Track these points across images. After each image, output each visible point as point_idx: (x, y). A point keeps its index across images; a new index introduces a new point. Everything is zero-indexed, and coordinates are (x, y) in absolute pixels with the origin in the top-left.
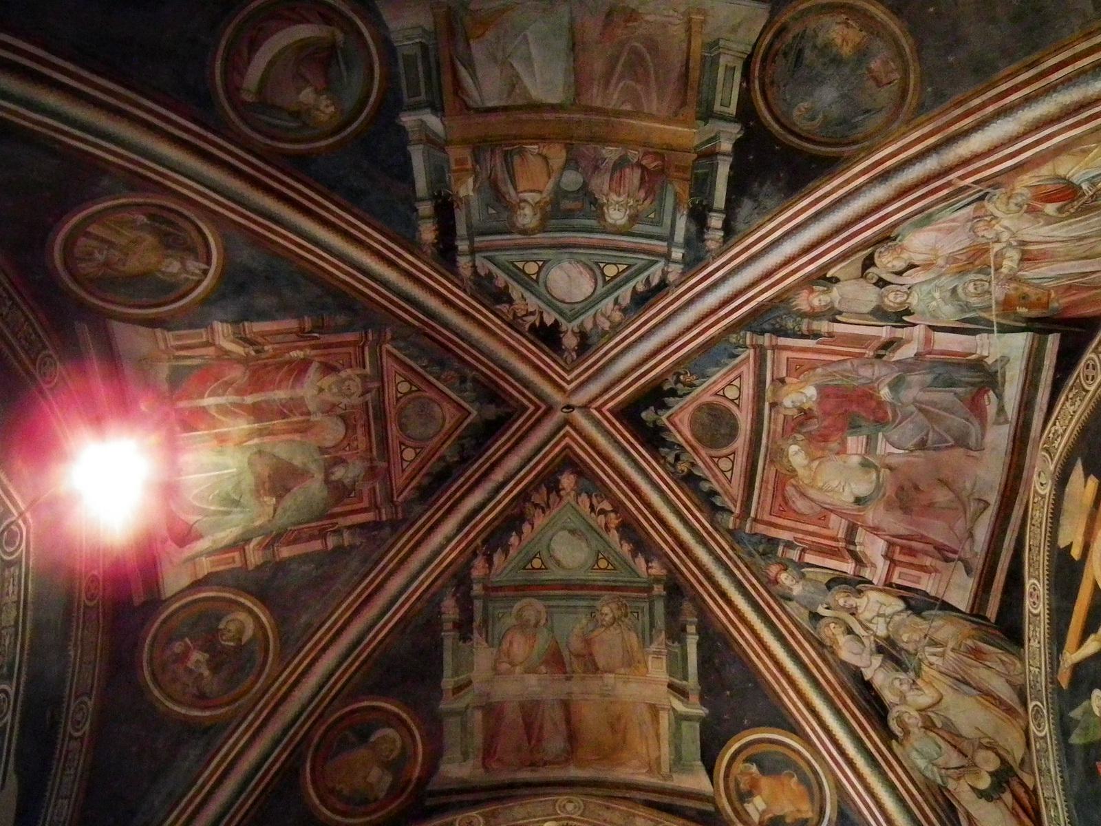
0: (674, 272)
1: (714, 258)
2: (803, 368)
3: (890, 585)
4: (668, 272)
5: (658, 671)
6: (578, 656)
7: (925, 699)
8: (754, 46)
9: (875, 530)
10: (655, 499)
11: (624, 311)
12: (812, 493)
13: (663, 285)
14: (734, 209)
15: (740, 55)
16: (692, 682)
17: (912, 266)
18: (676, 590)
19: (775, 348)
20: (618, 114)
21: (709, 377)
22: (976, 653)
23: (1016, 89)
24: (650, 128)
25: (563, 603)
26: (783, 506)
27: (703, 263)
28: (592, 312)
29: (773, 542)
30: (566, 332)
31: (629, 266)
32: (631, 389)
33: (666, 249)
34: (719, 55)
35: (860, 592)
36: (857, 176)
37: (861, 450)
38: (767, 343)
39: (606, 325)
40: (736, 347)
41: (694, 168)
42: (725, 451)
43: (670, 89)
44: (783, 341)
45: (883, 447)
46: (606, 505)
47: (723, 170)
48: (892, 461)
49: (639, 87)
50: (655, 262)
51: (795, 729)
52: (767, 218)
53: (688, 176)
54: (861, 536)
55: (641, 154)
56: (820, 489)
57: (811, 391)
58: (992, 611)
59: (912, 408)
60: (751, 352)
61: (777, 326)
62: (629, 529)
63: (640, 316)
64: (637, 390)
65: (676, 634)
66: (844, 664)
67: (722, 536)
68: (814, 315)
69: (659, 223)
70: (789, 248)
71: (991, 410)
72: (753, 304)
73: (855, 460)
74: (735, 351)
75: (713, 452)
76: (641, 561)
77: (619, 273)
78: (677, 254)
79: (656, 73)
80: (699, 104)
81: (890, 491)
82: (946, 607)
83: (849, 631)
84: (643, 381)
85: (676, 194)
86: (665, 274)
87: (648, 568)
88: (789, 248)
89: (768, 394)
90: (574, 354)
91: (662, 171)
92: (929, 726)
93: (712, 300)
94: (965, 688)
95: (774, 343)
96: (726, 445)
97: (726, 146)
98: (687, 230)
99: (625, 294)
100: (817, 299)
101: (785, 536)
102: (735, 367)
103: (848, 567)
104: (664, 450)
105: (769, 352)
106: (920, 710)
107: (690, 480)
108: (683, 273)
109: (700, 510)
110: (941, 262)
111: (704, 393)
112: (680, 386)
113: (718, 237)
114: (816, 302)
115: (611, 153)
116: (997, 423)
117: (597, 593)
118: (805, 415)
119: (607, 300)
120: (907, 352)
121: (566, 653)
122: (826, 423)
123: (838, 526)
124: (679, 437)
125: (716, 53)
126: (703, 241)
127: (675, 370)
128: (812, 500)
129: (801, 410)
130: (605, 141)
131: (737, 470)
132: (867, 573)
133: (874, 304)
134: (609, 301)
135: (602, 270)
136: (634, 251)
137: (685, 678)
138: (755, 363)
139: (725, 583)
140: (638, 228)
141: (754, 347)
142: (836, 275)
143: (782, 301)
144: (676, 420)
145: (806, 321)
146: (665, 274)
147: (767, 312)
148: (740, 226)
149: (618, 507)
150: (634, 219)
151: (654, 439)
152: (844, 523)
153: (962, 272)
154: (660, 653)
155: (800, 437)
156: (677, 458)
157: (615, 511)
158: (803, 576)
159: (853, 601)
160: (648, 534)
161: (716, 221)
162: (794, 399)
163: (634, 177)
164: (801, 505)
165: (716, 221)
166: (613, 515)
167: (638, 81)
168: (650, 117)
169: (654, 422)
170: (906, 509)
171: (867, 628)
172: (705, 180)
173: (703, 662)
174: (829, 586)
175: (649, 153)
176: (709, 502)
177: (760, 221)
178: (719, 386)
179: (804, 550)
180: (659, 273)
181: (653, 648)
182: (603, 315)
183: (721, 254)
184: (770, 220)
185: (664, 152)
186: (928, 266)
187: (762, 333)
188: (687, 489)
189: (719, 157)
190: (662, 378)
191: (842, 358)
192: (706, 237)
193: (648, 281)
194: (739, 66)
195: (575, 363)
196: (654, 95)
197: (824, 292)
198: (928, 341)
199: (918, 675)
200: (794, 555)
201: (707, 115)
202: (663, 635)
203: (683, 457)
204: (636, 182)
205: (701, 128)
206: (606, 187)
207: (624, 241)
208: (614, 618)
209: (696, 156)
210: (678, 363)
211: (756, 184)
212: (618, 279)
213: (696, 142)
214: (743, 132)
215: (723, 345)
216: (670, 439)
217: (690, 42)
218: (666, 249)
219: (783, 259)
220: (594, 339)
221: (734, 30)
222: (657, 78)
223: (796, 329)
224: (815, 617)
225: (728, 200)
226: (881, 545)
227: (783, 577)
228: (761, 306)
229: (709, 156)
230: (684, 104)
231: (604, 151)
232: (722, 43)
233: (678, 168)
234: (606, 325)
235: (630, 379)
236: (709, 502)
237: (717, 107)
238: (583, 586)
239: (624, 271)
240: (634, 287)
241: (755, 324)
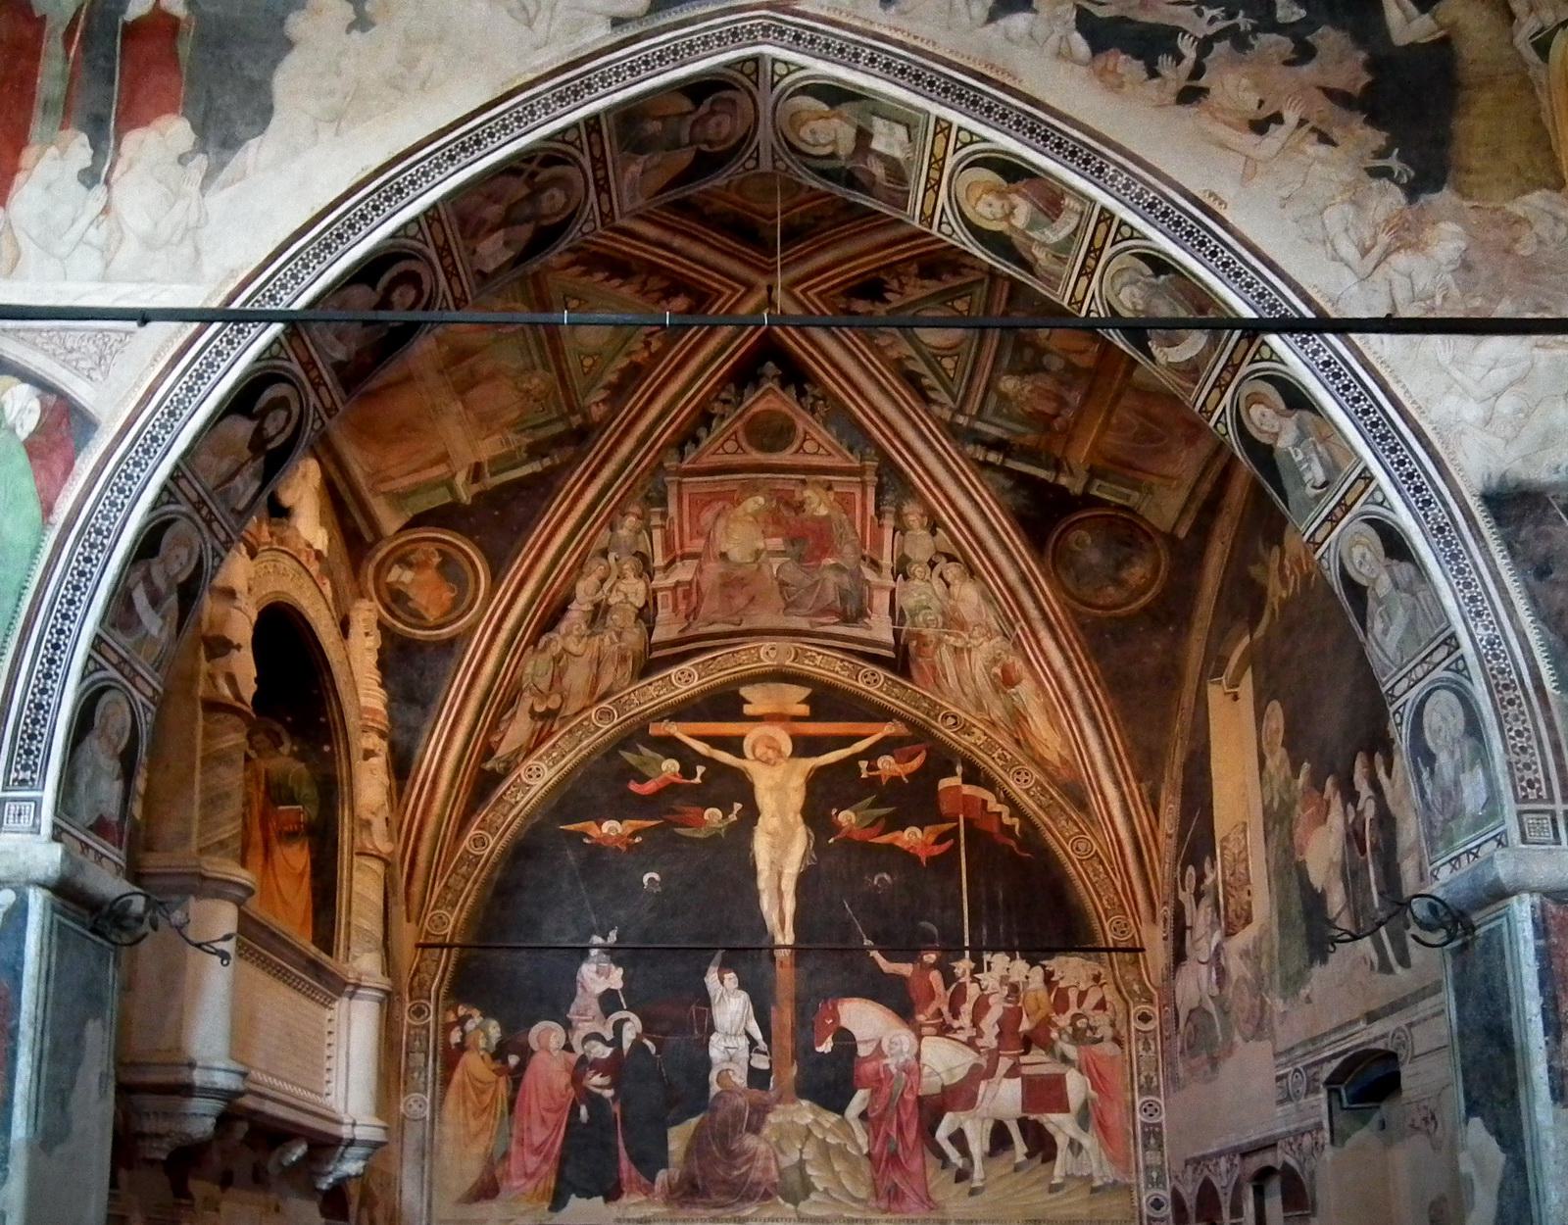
0: (947, 415)
3: (655, 591)
5: (488, 448)
6: (472, 372)
7: (573, 648)
9: (700, 570)
10: (674, 387)
11: (899, 361)
12: (721, 523)
13: (923, 395)
16: (491, 481)
17: (948, 585)
18: (582, 436)
19: (863, 484)
20: (1110, 412)
21: (825, 427)
22: (623, 659)
23: (1084, 671)
25: (532, 342)
26: (701, 503)
29: (663, 501)
31: (952, 380)
32: (800, 351)
35: (640, 576)
36: (1027, 565)
37: (770, 548)
38: (867, 478)
39: (883, 341)
42: (744, 444)
45: (776, 562)
46: (655, 345)
47: (1042, 474)
48: (765, 568)
50: (954, 400)
51: (496, 579)
54: (692, 564)
56: (727, 527)
57: (823, 511)
58: (656, 654)
59: (817, 577)
60: (857, 464)
62: (634, 374)
63: (892, 373)
64: (798, 357)
65: (535, 451)
66: (574, 588)
67: (654, 457)
68: (899, 516)
69: (997, 412)
70: (963, 504)
71: (824, 620)
72: (907, 469)
73: (761, 545)
74: (856, 451)
75: (741, 434)
76: (603, 394)
77: (944, 369)
78: (961, 420)
81: (739, 573)
82: (650, 631)
83: (603, 581)
84: (810, 362)
85: (1024, 435)
86: (942, 405)
87: (597, 404)
88: (963, 504)
89: (814, 478)
91: (1048, 427)
92: (556, 660)
93: (910, 435)
94: (595, 666)
96: (750, 444)
97: (1063, 481)
98: (987, 434)
99: (920, 367)
100: (913, 513)
101: (672, 510)
102: (839, 451)
103: (659, 561)
104: (731, 386)
106: (564, 649)
107: (704, 418)
108: (940, 418)
109: (675, 432)
110: (952, 602)
111: (803, 422)
112: (811, 400)
115: (1075, 398)
116: (811, 623)
117: (553, 367)
118: (799, 507)
120: (869, 574)
121: (471, 361)
122: (792, 523)
123: (698, 545)
124: (752, 400)
127: (827, 395)
128: (714, 523)
129: (802, 503)
131: (728, 458)
132: (658, 575)
133: (911, 556)
134: (913, 353)
137: (493, 474)
139: (606, 473)
140: (993, 399)
144: (770, 397)
146: (942, 405)
148: (987, 473)
149: (656, 357)
150: (1004, 397)
151: (744, 376)
152: (699, 550)
153: (943, 614)
154: (508, 442)
155: (774, 503)
156: (726, 402)
157: (651, 355)
158: (638, 532)
159: (630, 574)
160: (635, 392)
161: (992, 457)
163: (1049, 407)
164: (707, 516)
165: (992, 457)
166: (646, 354)
168: (1102, 432)
169: (762, 375)
170: (725, 585)
171: (611, 590)
173: (519, 483)
174: (637, 554)
176: (686, 439)
178: (816, 437)
179: (663, 527)
180: (941, 400)
181: (511, 436)
183: (960, 454)
184: (990, 495)
185: (1069, 435)
186: (949, 595)
187: (879, 475)
188: (693, 417)
190: (816, 381)
193: (933, 389)
197: (922, 525)
198: (882, 588)
199: (589, 636)
200: (656, 521)
201: (1093, 473)
202: (528, 441)
203: (728, 408)
207: (981, 382)
208: (528, 391)
210: (837, 399)
216: (746, 391)
224: (604, 553)
226: (688, 577)
227: (630, 521)
228: (906, 476)
229: (1057, 466)
235: (811, 349)
236: (686, 439)
237: (1098, 482)
238: (557, 352)
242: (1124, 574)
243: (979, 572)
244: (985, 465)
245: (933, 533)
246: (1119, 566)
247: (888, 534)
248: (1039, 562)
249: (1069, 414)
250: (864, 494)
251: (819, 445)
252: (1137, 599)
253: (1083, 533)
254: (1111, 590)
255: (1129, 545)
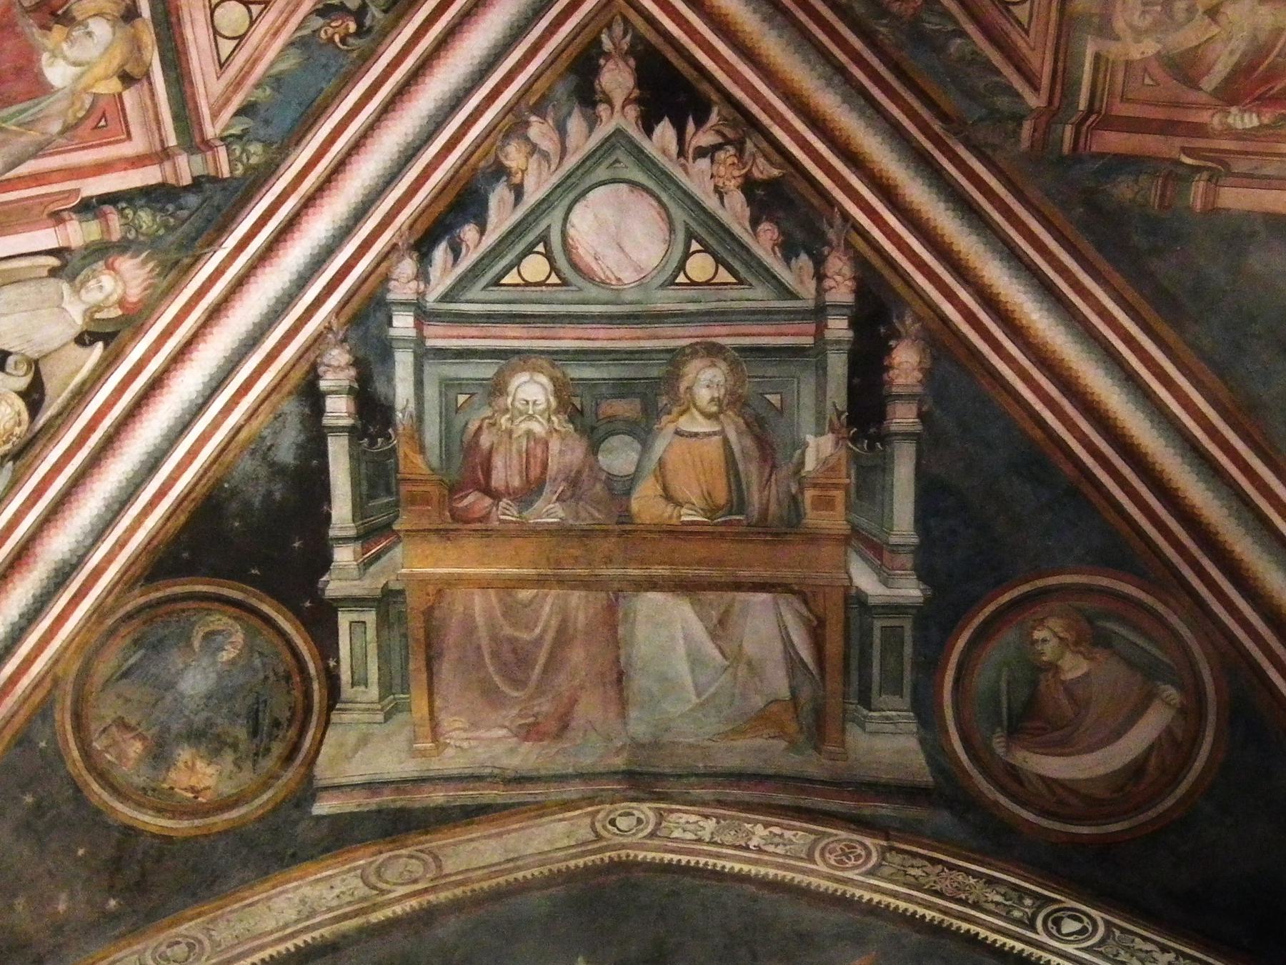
1: (329, 329)
2: (90, 123)
4: (416, 278)
8: (327, 722)
11: (500, 171)
13: (423, 246)
14: (309, 440)
15: (349, 706)
19: (163, 155)
20: (540, 582)
21: (291, 44)
24: (482, 564)
27: (349, 310)
28: (571, 161)
30: (627, 102)
33: (428, 331)
34: (381, 698)
38: (182, 160)
39: (538, 130)
40: (245, 131)
41: (397, 504)
43: (452, 637)
44: (149, 176)
47: (341, 510)
49: (508, 631)
50: (445, 298)
52: (243, 435)
53: (404, 489)
55: (493, 516)
57: (57, 73)
60: (211, 131)
61: (171, 207)
63: (465, 160)
68: (101, 252)
69: (449, 386)
78: (403, 323)
79: (481, 657)
80: (402, 618)
85: (422, 449)
86: (422, 275)
89: (148, 37)
90: (607, 44)
91: (455, 490)
93: (318, 228)
95: (168, 165)
97: (344, 556)
98: (390, 380)
102: (237, 84)
105: (172, 141)
108: (386, 279)
113: (329, 376)
114: (107, 281)
115: (548, 511)
119: (540, 195)
125: (386, 701)
126: (356, 363)
129: (67, 20)
130: (561, 532)
135: (554, 268)
136: (490, 318)
138: (196, 107)
140: (487, 370)
141: (207, 145)
142: (88, 350)
143: (177, 262)
145: (116, 236)
146: (422, 275)
147: (199, 233)
148: (292, 408)
150: (497, 388)
161: (339, 409)
162: (88, 42)
163: (504, 473)
165: (339, 409)
167: (512, 640)
168: (484, 584)
172: (372, 486)
175: (480, 520)
177: (255, 424)
180: (435, 272)
182: (545, 156)
183: (318, 338)
184: (238, 430)
187: (198, 183)
189: (352, 533)
191: (23, 169)
192: (352, 372)
193: (456, 251)
194: (347, 691)
195: (603, 19)
196: (480, 620)
197: (99, 308)
204: (498, 462)
205: (393, 577)
206: (555, 446)
209: (395, 527)
210: (367, 58)
211: (278, 496)
212: (520, 247)
213: (398, 552)
214: (320, 585)
215: (272, 132)
217: (431, 712)
218: (428, 331)
219: (195, 355)
220: (561, 91)
221: (364, 741)
222: (479, 647)
223: (129, 212)
225: (323, 455)
230: (428, 613)
231: (562, 514)
232: (380, 717)
233: (426, 500)
234: (538, 130)
237: (370, 617)
239: (506, 271)
240: (482, 232)
241: (218, 198)
242: (184, 754)
243: (30, 468)
244: (312, 396)
245: (84, 339)
246: (195, 736)
247: (46, 238)
248: (127, 582)
249: (507, 512)
250: (137, 162)
251: (240, 39)
252: (140, 805)
253: (239, 638)
254: (135, 748)
255: (254, 732)
